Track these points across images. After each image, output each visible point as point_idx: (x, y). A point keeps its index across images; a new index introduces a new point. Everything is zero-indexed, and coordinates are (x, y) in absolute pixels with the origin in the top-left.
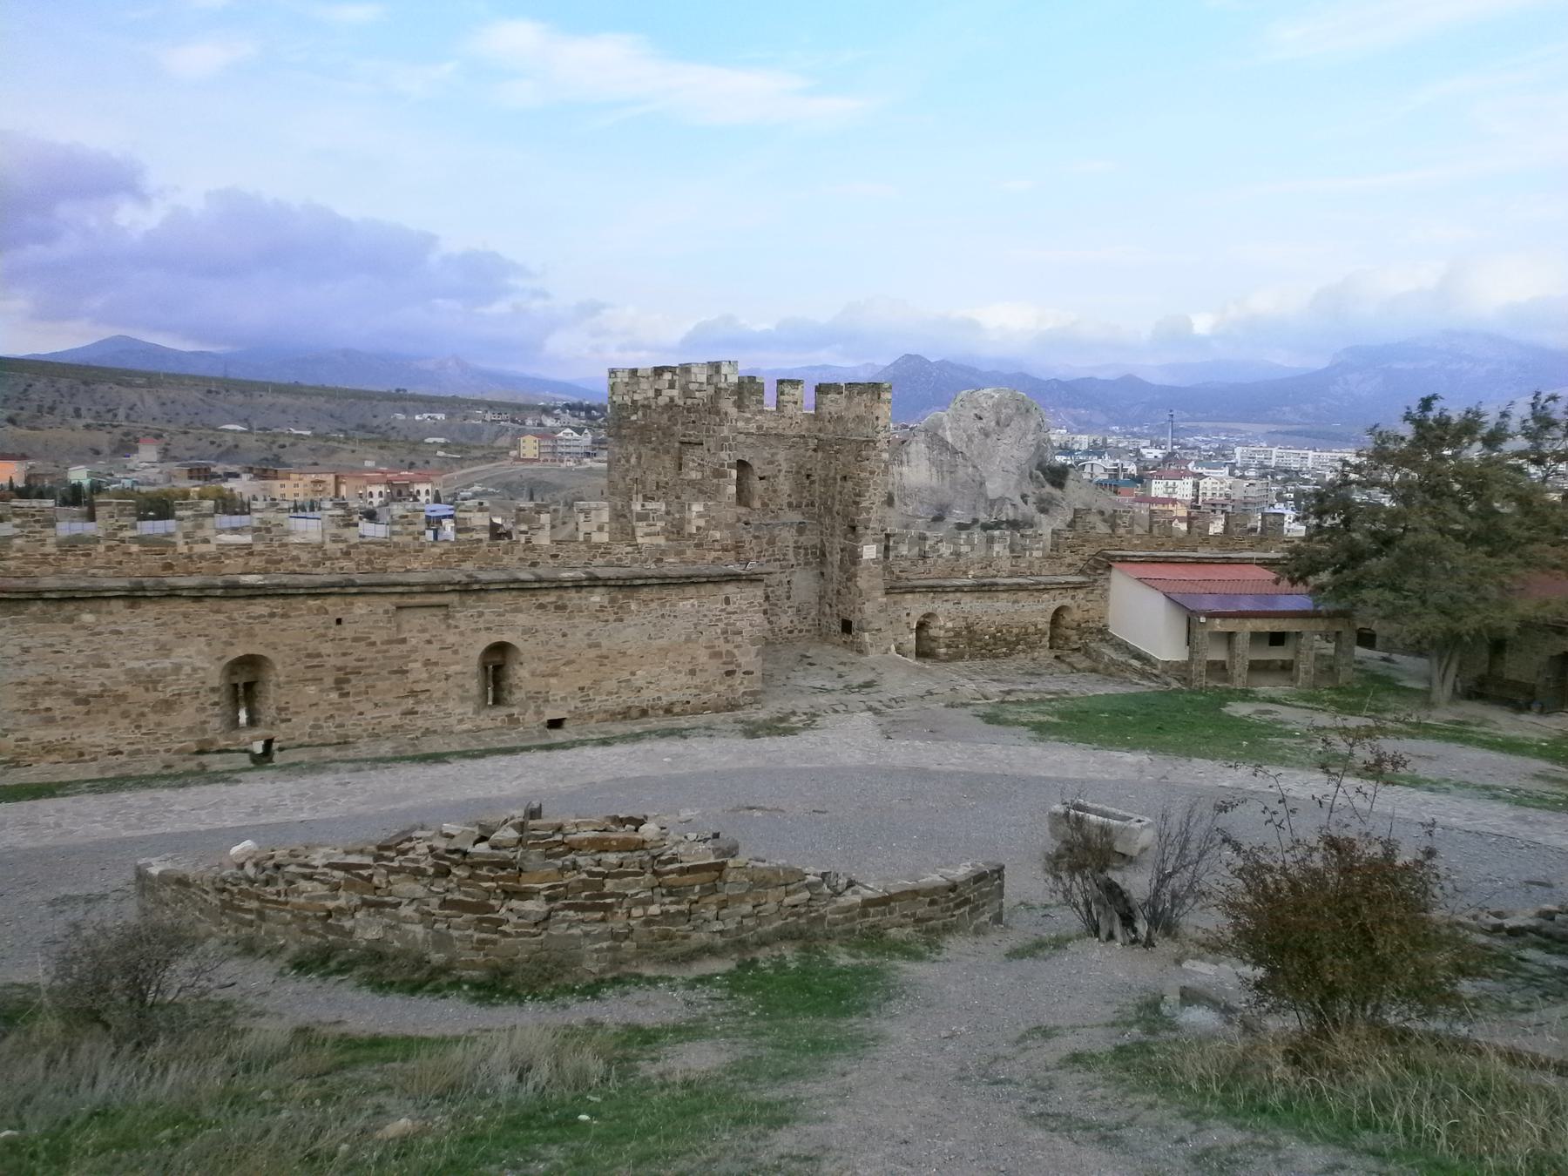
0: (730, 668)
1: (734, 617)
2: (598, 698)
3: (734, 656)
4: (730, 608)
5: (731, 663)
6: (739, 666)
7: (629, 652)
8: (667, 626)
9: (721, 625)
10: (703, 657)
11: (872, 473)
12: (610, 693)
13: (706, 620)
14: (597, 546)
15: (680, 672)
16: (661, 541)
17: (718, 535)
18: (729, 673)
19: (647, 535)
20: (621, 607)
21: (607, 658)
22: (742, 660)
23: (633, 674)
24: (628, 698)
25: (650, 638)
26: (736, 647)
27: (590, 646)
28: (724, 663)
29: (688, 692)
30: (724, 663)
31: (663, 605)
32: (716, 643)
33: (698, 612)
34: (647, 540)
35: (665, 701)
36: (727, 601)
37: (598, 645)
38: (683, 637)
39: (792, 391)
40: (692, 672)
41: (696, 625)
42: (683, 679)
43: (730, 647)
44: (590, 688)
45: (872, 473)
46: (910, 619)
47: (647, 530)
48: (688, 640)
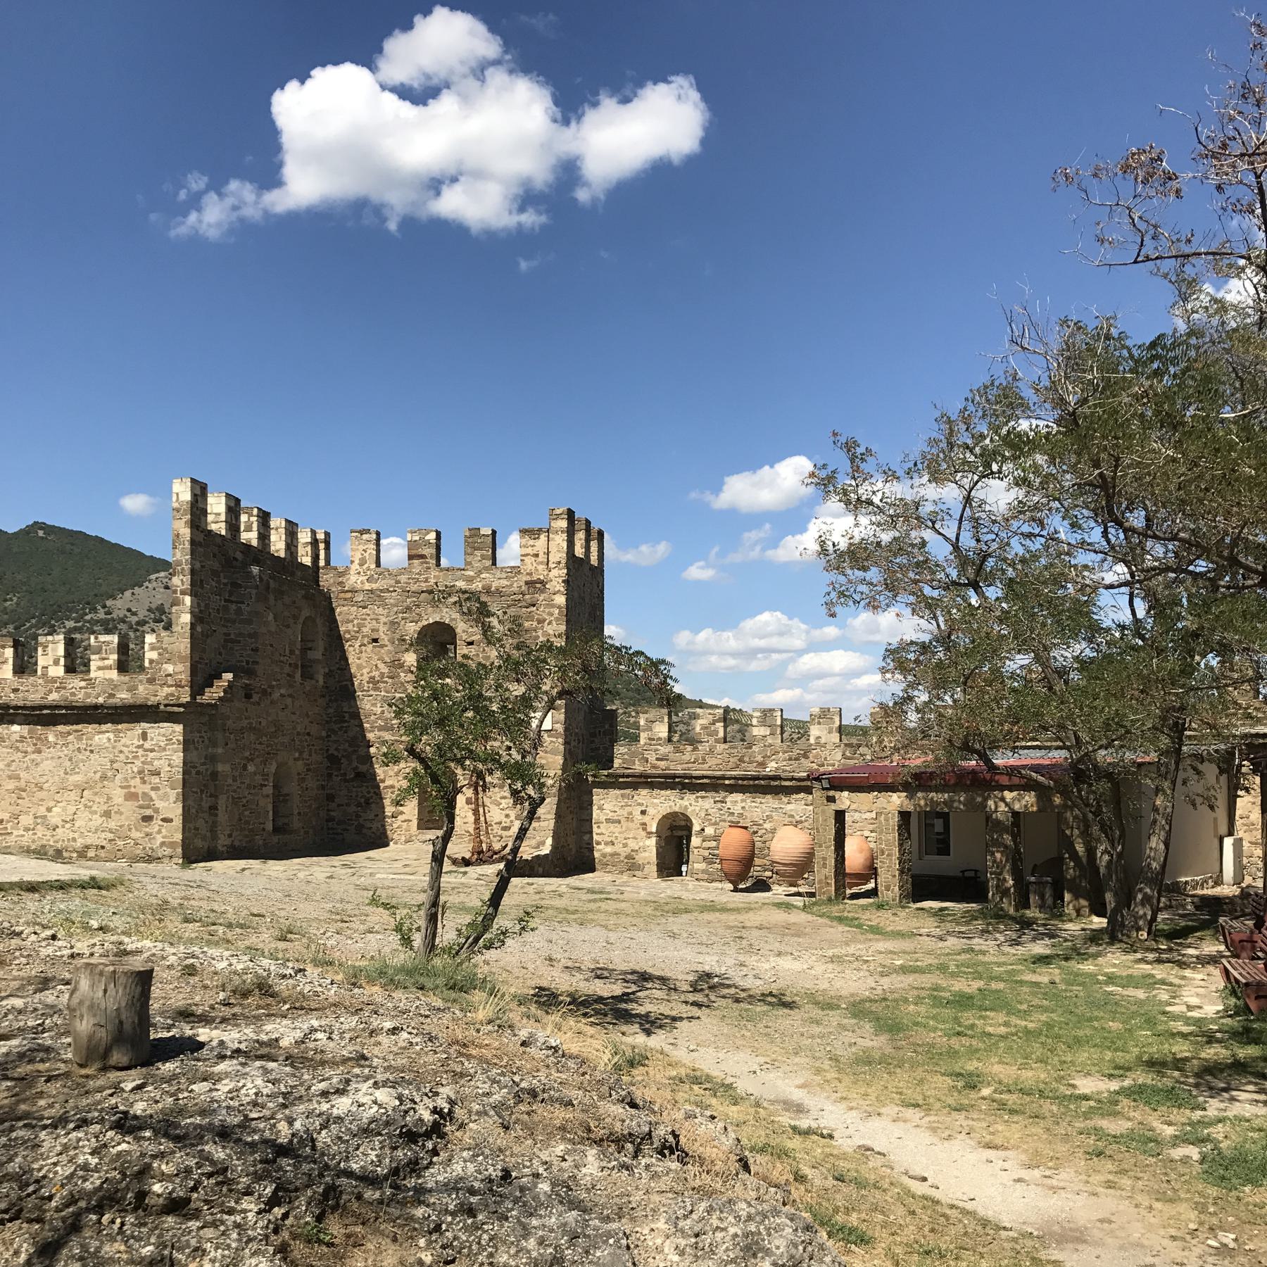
0: (148, 812)
1: (151, 755)
2: (16, 833)
3: (152, 800)
4: (147, 745)
5: (148, 807)
6: (157, 811)
7: (46, 786)
8: (83, 761)
9: (138, 763)
10: (118, 795)
11: (541, 621)
12: (26, 829)
13: (122, 757)
14: (54, 680)
15: (95, 812)
16: (114, 674)
17: (170, 668)
18: (147, 819)
19: (100, 668)
20: (39, 739)
21: (24, 791)
22: (159, 804)
23: (49, 810)
24: (42, 836)
25: (66, 773)
26: (153, 789)
27: (10, 777)
28: (141, 807)
29: (103, 836)
30: (141, 807)
31: (79, 739)
32: (132, 783)
33: (114, 748)
34: (100, 674)
35: (79, 844)
36: (144, 736)
37: (18, 778)
38: (99, 775)
39: (531, 542)
40: (107, 814)
41: (112, 762)
42: (98, 820)
43: (147, 788)
44: (8, 822)
45: (541, 621)
46: (646, 819)
47: (100, 663)
48: (104, 777)
